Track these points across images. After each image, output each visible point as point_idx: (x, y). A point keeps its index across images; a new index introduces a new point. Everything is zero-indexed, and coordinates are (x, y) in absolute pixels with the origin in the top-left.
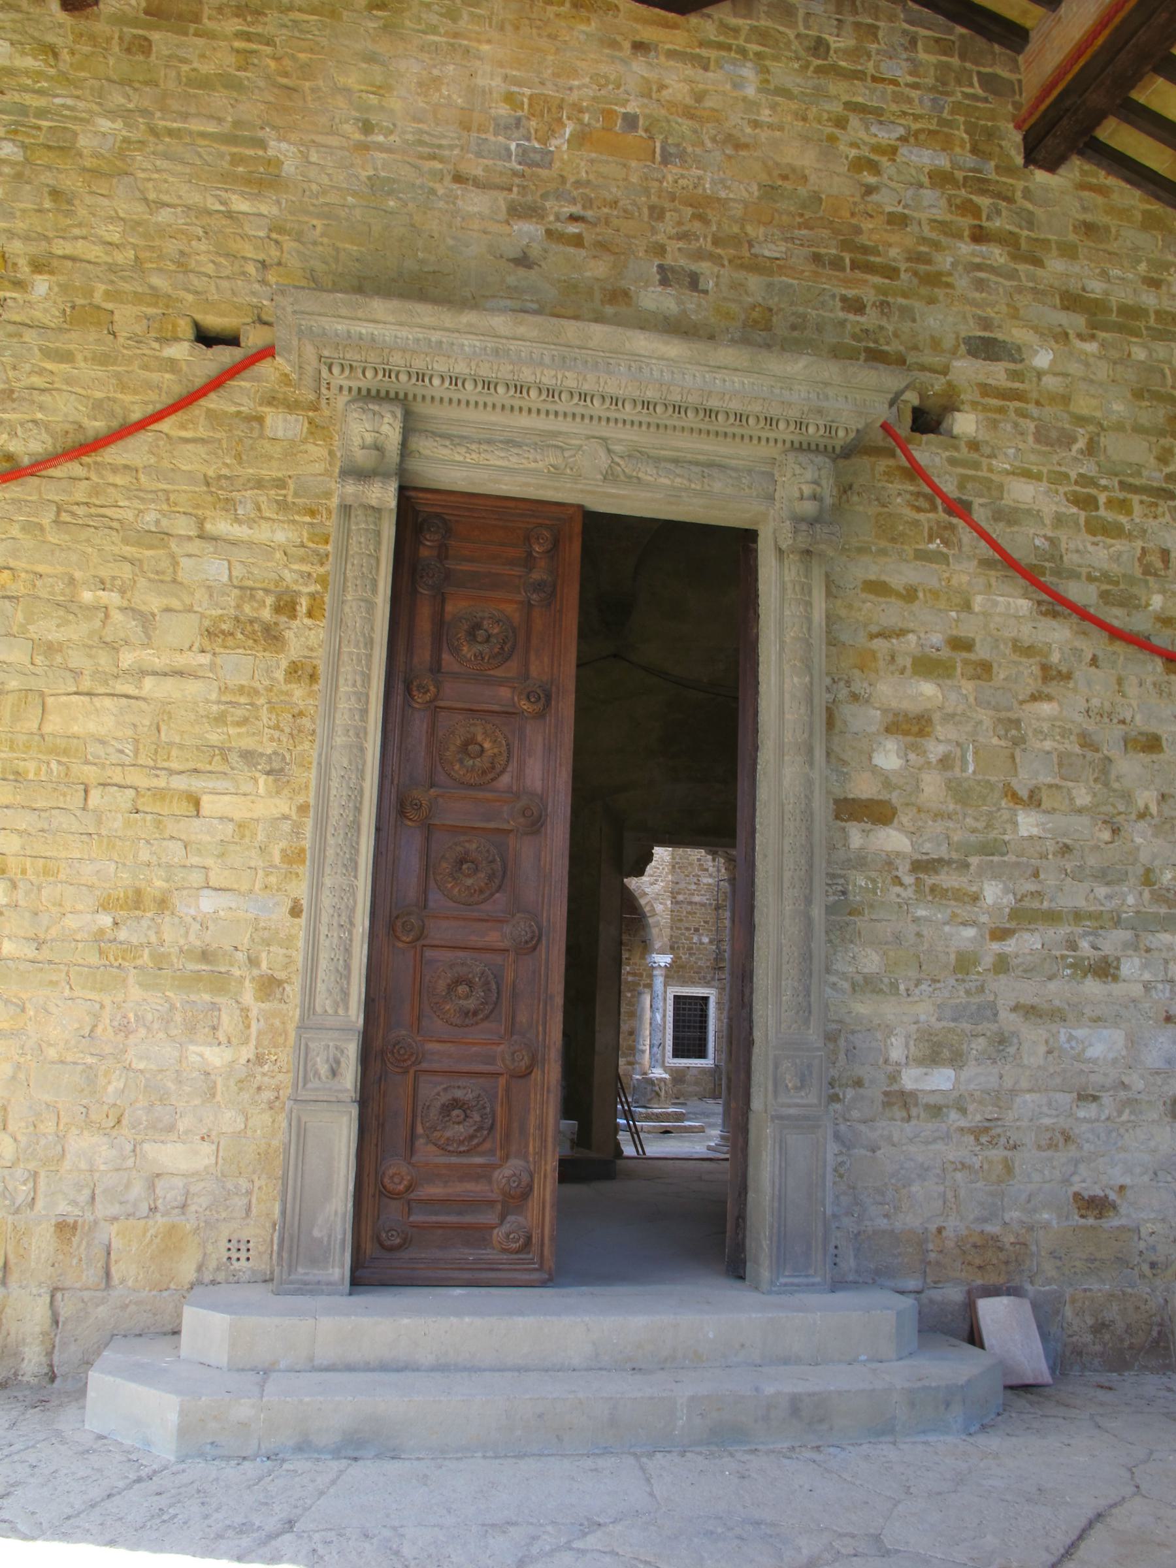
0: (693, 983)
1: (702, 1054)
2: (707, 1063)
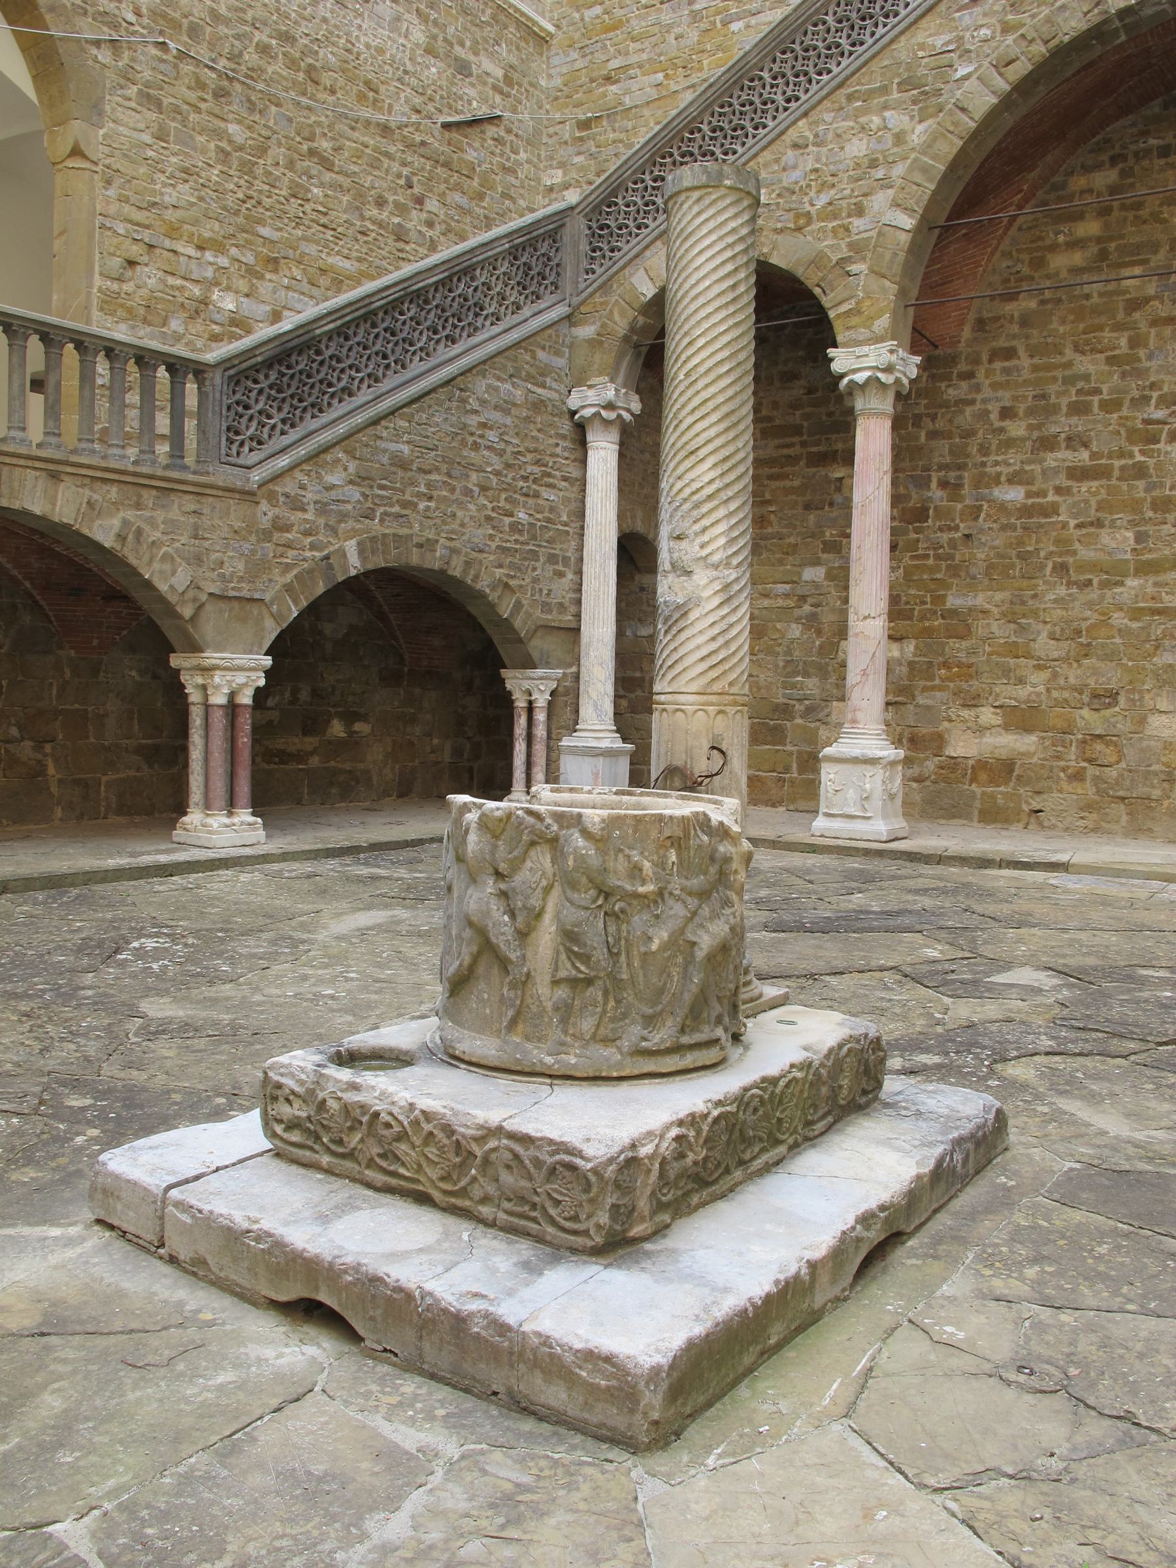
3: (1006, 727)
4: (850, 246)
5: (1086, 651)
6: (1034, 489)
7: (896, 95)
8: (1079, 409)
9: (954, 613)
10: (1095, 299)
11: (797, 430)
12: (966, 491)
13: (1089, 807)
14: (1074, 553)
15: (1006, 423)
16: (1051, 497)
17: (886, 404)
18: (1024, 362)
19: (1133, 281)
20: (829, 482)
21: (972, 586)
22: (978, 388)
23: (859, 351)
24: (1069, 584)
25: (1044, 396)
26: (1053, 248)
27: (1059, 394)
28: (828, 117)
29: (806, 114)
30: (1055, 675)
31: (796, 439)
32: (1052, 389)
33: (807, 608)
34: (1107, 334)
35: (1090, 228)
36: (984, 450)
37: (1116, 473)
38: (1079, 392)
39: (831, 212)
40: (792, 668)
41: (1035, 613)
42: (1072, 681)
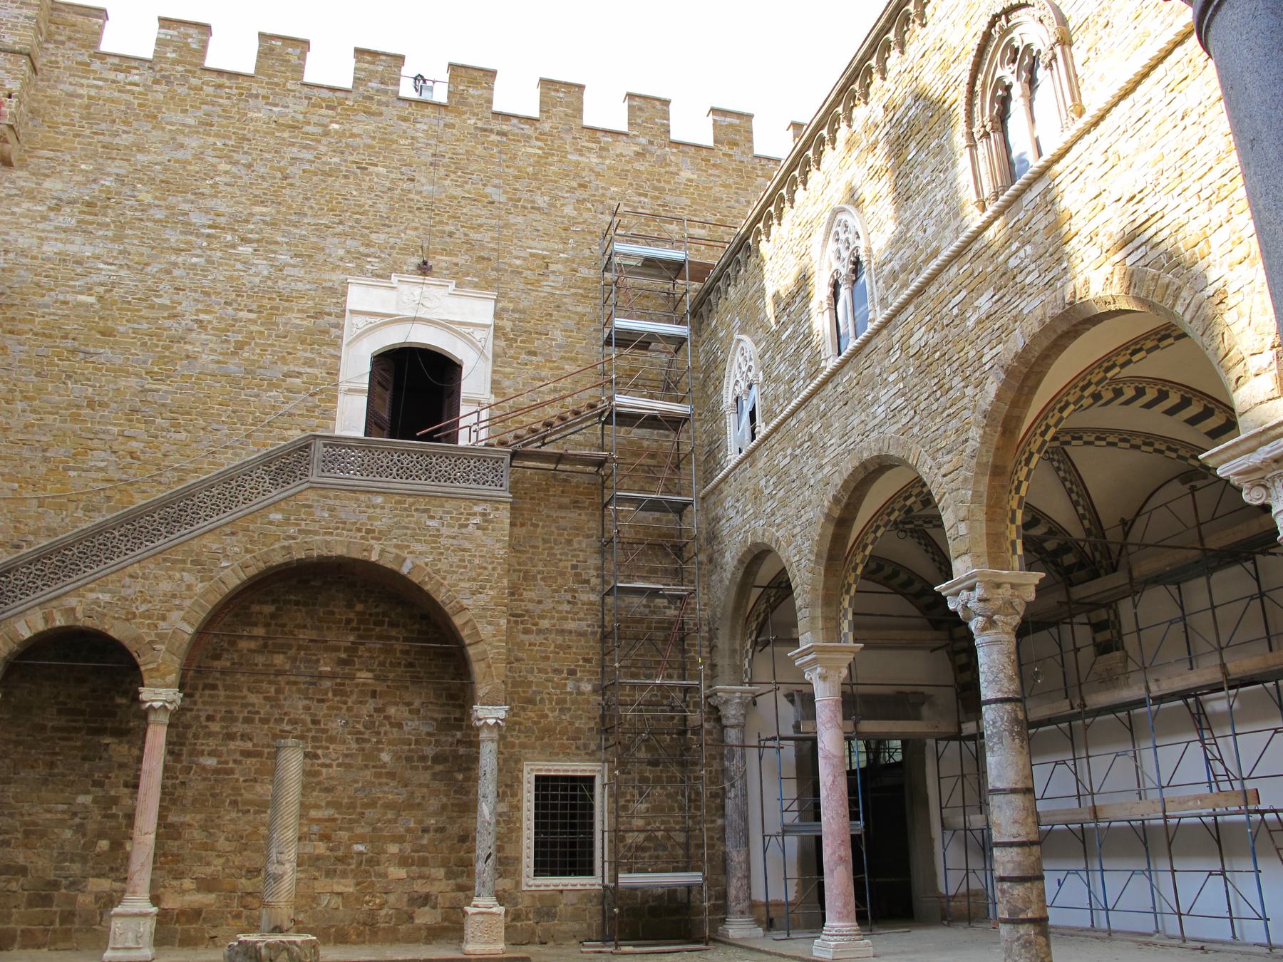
0: (565, 753)
3: (198, 890)
4: (157, 635)
5: (245, 847)
7: (189, 566)
8: (248, 720)
9: (172, 825)
10: (260, 667)
11: (82, 713)
12: (184, 758)
16: (231, 765)
17: (165, 719)
18: (222, 693)
19: (279, 659)
21: (184, 809)
22: (195, 703)
23: (157, 690)
25: (230, 712)
26: (241, 637)
27: (239, 712)
28: (152, 566)
29: (139, 562)
30: (228, 860)
31: (81, 718)
32: (236, 708)
33: (77, 820)
34: (265, 685)
35: (260, 631)
36: (196, 736)
39: (147, 615)
40: (63, 857)
41: (218, 827)
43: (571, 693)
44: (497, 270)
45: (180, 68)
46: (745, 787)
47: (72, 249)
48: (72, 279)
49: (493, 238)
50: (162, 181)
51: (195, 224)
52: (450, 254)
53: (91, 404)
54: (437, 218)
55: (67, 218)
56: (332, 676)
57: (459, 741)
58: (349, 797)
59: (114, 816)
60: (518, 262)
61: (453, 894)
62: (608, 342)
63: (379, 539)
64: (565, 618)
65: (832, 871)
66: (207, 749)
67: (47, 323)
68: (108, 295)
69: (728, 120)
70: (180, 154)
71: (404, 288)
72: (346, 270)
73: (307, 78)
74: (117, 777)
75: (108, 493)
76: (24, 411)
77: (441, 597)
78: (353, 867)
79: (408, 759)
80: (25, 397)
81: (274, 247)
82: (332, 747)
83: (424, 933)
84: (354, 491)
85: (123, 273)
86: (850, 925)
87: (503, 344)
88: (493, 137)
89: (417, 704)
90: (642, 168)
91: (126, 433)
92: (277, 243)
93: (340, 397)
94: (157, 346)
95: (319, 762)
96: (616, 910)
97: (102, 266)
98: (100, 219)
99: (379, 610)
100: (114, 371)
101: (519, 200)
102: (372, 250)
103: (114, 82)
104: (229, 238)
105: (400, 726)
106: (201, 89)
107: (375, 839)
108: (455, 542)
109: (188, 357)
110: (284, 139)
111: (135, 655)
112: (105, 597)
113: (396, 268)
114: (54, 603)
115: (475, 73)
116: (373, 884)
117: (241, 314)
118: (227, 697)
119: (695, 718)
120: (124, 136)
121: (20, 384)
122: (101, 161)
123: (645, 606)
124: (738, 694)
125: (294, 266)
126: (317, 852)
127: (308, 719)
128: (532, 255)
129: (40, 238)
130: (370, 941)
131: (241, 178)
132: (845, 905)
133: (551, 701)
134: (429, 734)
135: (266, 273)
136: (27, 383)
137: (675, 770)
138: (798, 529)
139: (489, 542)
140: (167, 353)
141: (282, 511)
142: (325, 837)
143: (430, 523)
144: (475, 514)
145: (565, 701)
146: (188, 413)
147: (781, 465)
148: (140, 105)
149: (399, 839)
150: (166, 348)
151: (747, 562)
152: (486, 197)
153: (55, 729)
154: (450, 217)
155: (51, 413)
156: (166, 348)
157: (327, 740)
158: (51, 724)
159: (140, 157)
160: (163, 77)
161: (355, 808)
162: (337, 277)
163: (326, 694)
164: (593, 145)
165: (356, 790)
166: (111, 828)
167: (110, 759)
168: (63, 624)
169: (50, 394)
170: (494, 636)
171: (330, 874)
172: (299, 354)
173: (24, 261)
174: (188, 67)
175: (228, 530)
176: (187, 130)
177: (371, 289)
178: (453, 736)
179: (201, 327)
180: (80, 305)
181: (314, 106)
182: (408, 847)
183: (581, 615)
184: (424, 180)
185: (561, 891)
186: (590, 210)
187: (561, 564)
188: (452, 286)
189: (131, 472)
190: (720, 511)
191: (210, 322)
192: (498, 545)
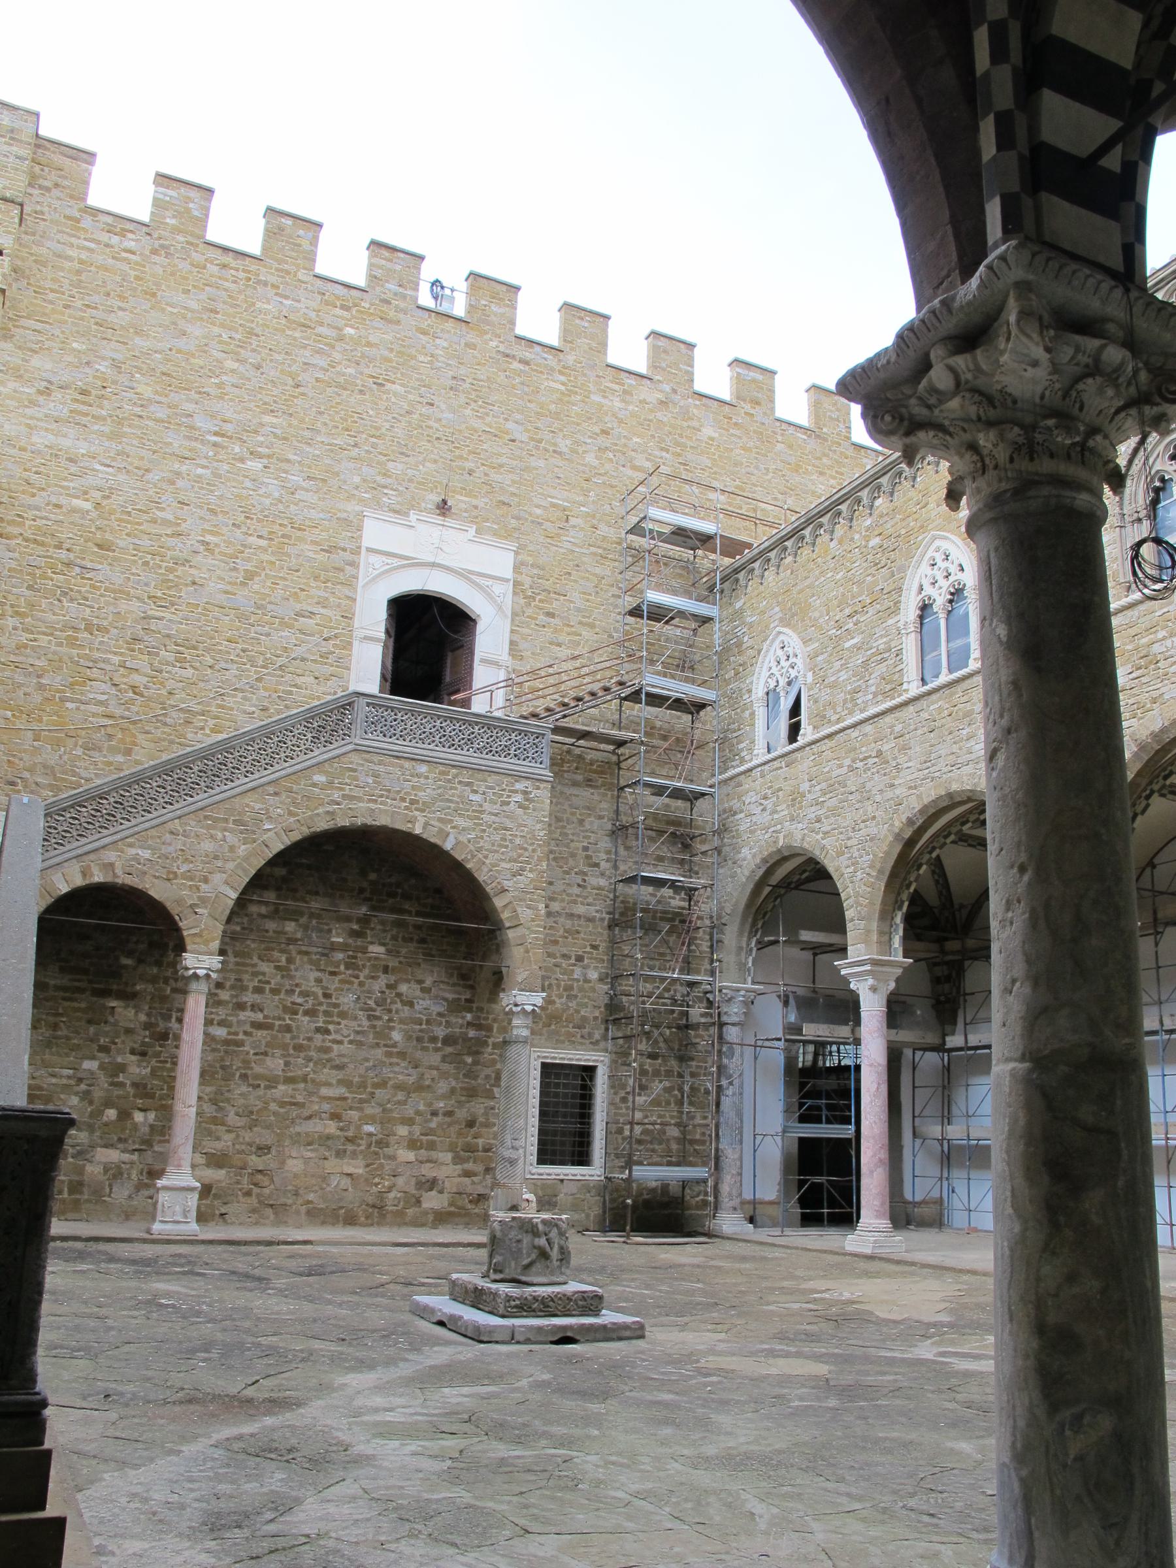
1: (582, 1157)
2: (593, 1172)
3: (208, 1165)
4: (199, 897)
6: (232, 1030)
8: (259, 990)
10: (271, 934)
13: (254, 1211)
14: (252, 1069)
15: (219, 991)
16: (241, 1036)
17: (203, 987)
19: (290, 927)
20: (105, 1007)
24: (249, 1085)
25: (240, 980)
28: (193, 823)
30: (238, 1136)
31: (85, 977)
32: (246, 977)
33: (83, 1087)
37: (276, 1028)
38: (260, 981)
39: (189, 876)
41: (228, 1100)
42: (247, 1139)
43: (578, 980)
44: (518, 518)
45: (181, 238)
46: (741, 1086)
47: (66, 443)
48: (65, 479)
49: (514, 482)
50: (164, 374)
51: (199, 429)
52: (469, 494)
53: (89, 628)
54: (457, 452)
55: (59, 404)
56: (344, 947)
57: (469, 1024)
58: (361, 1076)
59: (121, 1085)
60: (538, 511)
61: (459, 1179)
62: (636, 612)
63: (423, 811)
64: (575, 902)
65: (871, 1172)
66: (217, 1018)
67: (39, 528)
68: (105, 503)
69: (751, 374)
70: (181, 343)
71: (421, 527)
72: (361, 501)
73: (320, 269)
74: (123, 1042)
75: (109, 731)
76: (15, 629)
77: (482, 877)
78: (363, 1148)
79: (419, 1039)
80: (17, 613)
81: (284, 466)
82: (343, 1022)
83: (431, 1217)
84: (397, 757)
85: (122, 477)
86: (885, 1223)
87: (522, 601)
88: (516, 365)
89: (428, 982)
90: (665, 419)
91: (128, 664)
92: (288, 461)
93: (356, 644)
94: (160, 567)
95: (330, 1038)
96: (629, 1201)
97: (98, 467)
98: (95, 411)
99: (393, 880)
100: (114, 591)
101: (540, 441)
102: (389, 481)
103: (107, 245)
104: (237, 449)
105: (411, 1004)
106: (205, 267)
107: (385, 1120)
108: (497, 819)
109: (194, 583)
110: (295, 339)
111: (177, 918)
112: (146, 854)
113: (413, 504)
114: (92, 857)
115: (499, 287)
116: (382, 1166)
117: (253, 540)
118: (237, 964)
119: (697, 1013)
120: (120, 313)
121: (10, 597)
122: (94, 340)
123: (651, 895)
124: (742, 993)
125: (307, 490)
126: (327, 1131)
127: (320, 992)
128: (554, 505)
129: (29, 426)
130: (379, 1224)
131: (249, 379)
132: (882, 1204)
133: (558, 986)
134: (440, 1014)
135: (276, 494)
136: (18, 596)
137: (673, 1063)
138: (854, 842)
139: (530, 822)
140: (171, 577)
141: (326, 773)
142: (335, 1116)
143: (473, 797)
144: (516, 792)
145: (571, 988)
146: (195, 648)
147: (834, 774)
148: (137, 278)
149: (409, 1122)
150: (170, 570)
151: (771, 862)
152: (507, 433)
153: (58, 988)
154: (470, 452)
155: (44, 634)
156: (170, 570)
157: (338, 1016)
158: (52, 982)
159: (138, 340)
160: (162, 246)
161: (365, 1087)
162: (352, 507)
163: (338, 967)
164: (617, 387)
165: (367, 1069)
166: (118, 1097)
167: (115, 1024)
168: (102, 880)
169: (43, 611)
170: (533, 920)
171: (340, 1154)
172: (313, 592)
173: (12, 452)
174: (190, 239)
175: (271, 789)
176: (189, 315)
177: (387, 525)
178: (463, 1018)
179: (207, 550)
180: (74, 510)
181: (327, 303)
182: (417, 1130)
183: (590, 900)
184: (443, 407)
185: (562, 1181)
186: (611, 460)
187: (572, 845)
188: (472, 531)
189: (134, 709)
190: (735, 804)
191: (217, 545)
192: (539, 826)
